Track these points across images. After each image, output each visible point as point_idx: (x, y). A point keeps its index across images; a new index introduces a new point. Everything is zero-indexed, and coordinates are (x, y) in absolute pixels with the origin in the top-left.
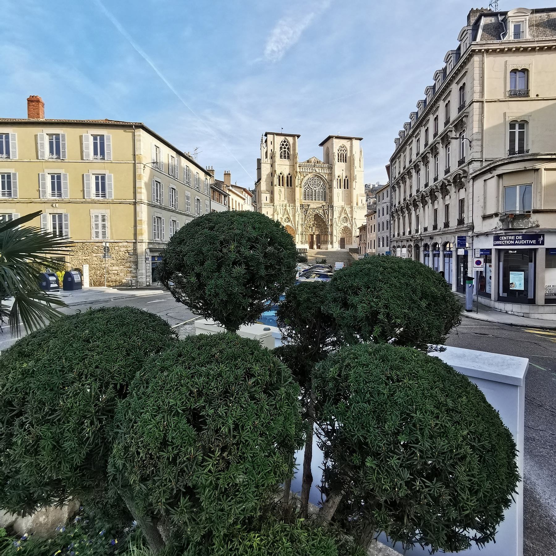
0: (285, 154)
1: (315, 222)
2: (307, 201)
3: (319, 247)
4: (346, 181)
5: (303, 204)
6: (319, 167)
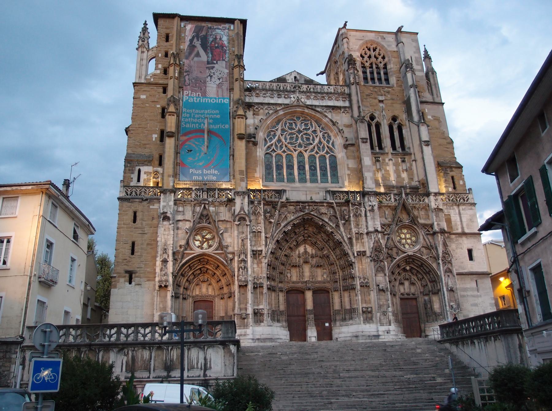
1: (309, 249)
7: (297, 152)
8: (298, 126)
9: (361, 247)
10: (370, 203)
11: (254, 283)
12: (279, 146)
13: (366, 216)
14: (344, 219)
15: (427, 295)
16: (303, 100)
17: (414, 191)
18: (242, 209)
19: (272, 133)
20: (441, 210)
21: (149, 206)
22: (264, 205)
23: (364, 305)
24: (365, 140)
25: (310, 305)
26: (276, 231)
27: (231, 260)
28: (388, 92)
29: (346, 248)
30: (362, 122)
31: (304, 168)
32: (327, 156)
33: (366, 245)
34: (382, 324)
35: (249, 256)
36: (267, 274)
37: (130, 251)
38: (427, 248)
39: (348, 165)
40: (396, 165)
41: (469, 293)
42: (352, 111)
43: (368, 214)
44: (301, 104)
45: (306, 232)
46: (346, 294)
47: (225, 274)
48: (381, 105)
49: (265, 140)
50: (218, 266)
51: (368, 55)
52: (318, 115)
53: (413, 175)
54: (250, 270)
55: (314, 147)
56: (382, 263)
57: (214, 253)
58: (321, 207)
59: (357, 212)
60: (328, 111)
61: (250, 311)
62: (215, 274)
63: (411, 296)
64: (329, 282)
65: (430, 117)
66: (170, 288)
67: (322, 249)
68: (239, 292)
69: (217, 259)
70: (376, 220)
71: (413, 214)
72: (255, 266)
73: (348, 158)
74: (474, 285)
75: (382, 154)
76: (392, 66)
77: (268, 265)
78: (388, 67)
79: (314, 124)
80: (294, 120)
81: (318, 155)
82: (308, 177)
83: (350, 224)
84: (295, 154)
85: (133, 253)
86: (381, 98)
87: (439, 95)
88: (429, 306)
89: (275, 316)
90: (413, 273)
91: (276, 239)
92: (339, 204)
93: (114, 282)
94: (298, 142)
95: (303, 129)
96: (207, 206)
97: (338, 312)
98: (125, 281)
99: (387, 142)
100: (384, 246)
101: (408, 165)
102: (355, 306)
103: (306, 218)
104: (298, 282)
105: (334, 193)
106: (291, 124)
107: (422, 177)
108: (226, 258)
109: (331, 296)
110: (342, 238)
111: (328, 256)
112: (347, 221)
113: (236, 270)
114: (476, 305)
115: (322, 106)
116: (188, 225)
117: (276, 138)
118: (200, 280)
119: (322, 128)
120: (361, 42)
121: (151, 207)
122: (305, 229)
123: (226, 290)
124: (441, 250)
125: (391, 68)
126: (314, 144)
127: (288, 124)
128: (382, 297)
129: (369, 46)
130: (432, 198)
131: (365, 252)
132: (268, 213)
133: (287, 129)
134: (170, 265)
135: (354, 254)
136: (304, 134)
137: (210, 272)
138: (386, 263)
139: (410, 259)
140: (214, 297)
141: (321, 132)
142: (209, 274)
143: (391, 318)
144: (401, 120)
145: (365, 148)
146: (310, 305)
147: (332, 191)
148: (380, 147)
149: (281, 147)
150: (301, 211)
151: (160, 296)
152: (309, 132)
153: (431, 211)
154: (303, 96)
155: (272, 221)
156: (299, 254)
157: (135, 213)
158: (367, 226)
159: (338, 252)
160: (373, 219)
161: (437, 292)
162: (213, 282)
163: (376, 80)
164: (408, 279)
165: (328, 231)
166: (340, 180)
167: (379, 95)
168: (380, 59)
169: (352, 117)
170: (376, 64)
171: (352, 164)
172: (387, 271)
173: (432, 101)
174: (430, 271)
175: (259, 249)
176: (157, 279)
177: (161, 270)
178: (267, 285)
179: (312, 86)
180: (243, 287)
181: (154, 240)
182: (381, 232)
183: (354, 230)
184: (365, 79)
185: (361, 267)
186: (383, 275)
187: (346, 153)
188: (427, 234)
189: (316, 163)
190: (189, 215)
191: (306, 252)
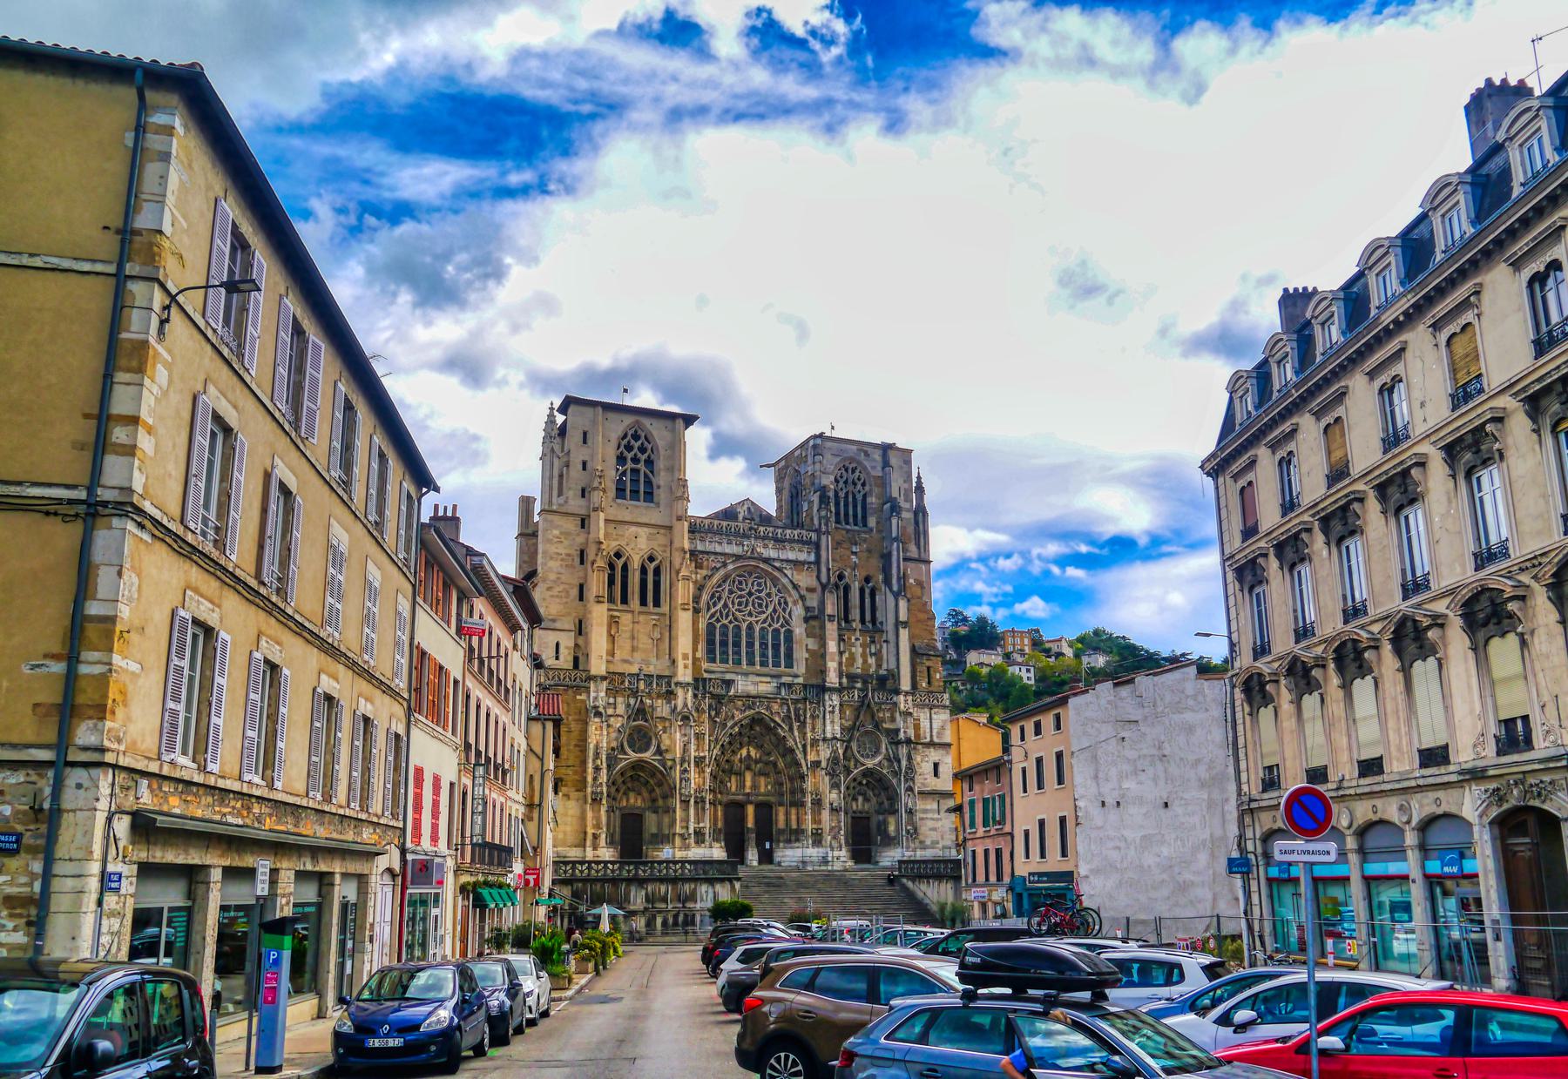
0: (635, 481)
1: (753, 753)
3: (766, 857)
4: (867, 591)
5: (706, 675)
6: (764, 538)
11: (696, 797)
17: (882, 681)
18: (685, 705)
20: (911, 714)
25: (750, 823)
30: (831, 592)
33: (822, 753)
38: (889, 760)
40: (863, 646)
41: (930, 816)
42: (819, 571)
43: (828, 716)
46: (793, 811)
52: (776, 574)
61: (691, 830)
65: (911, 581)
66: (604, 802)
73: (808, 636)
74: (935, 806)
78: (869, 500)
82: (757, 659)
84: (744, 626)
87: (926, 550)
92: (796, 701)
97: (781, 832)
99: (855, 614)
105: (790, 686)
106: (740, 583)
107: (893, 666)
114: (934, 829)
116: (617, 723)
117: (722, 602)
119: (779, 591)
120: (838, 459)
122: (752, 729)
123: (660, 802)
124: (904, 763)
129: (847, 464)
130: (902, 698)
131: (819, 762)
133: (735, 589)
134: (604, 772)
139: (868, 773)
140: (644, 810)
143: (843, 842)
145: (831, 629)
146: (750, 823)
148: (847, 620)
149: (727, 616)
152: (763, 595)
159: (789, 758)
160: (832, 722)
161: (894, 812)
163: (851, 520)
166: (795, 664)
168: (859, 484)
169: (818, 577)
171: (812, 644)
173: (917, 556)
176: (589, 790)
177: (595, 779)
179: (771, 529)
180: (685, 803)
183: (809, 735)
184: (837, 514)
190: (621, 709)
191: (749, 755)
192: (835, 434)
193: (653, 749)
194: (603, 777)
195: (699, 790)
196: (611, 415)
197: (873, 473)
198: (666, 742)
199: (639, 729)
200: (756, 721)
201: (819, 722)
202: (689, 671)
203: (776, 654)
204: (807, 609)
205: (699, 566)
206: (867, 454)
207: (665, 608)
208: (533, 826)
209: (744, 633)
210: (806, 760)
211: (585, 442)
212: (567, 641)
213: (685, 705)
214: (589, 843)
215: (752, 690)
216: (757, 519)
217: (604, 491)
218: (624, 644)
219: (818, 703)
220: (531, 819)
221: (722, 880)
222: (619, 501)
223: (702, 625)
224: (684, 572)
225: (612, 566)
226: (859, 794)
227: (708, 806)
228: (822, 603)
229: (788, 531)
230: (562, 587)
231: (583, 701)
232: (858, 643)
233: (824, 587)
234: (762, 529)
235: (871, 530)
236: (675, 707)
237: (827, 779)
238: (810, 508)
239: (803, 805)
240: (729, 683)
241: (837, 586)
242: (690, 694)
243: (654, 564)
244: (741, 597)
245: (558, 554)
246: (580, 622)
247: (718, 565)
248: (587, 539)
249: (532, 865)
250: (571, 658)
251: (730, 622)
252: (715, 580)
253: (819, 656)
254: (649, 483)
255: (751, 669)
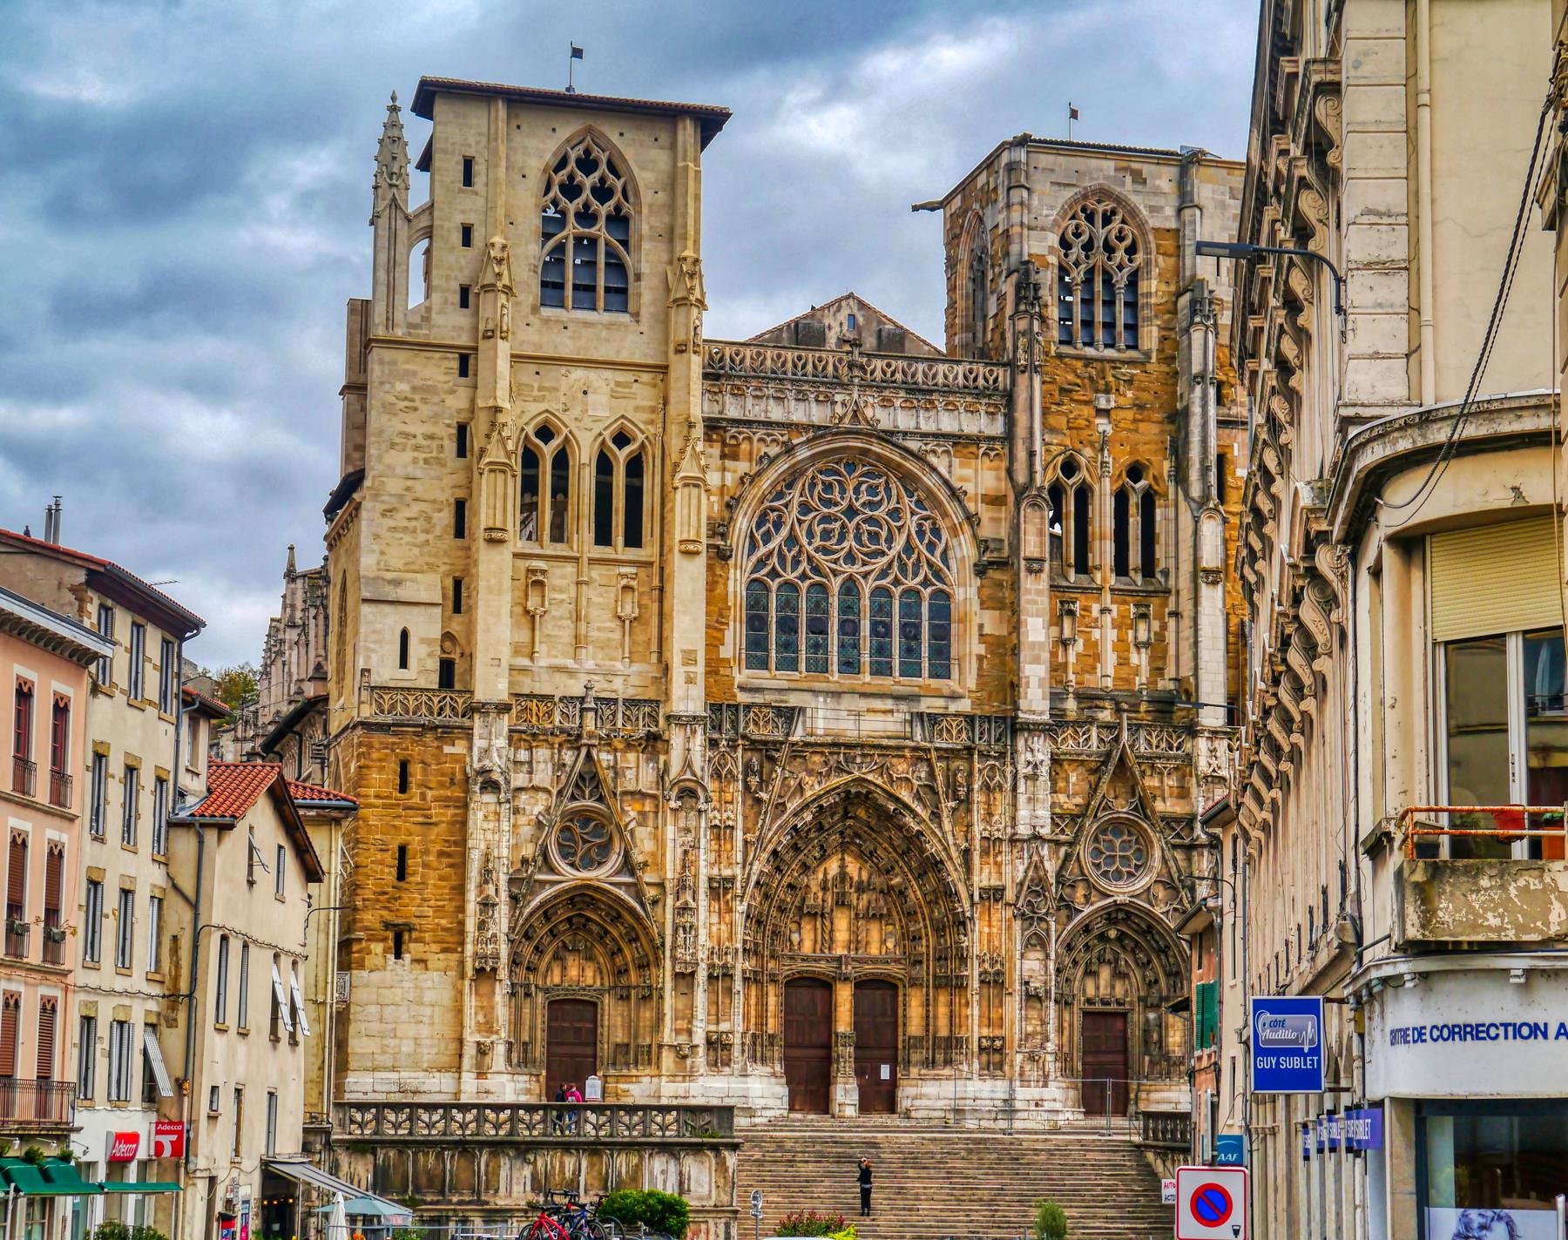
1: (853, 868)
2: (770, 677)
3: (880, 1098)
4: (1134, 500)
5: (743, 698)
7: (840, 579)
8: (850, 493)
9: (994, 876)
10: (1029, 757)
11: (712, 966)
12: (789, 556)
13: (1014, 788)
14: (956, 798)
15: (1155, 1007)
16: (869, 413)
18: (688, 764)
19: (773, 516)
20: (1223, 779)
21: (440, 748)
22: (744, 750)
23: (985, 1032)
24: (1036, 566)
25: (844, 1022)
26: (773, 821)
27: (655, 902)
28: (1130, 382)
29: (955, 875)
31: (856, 629)
32: (926, 592)
33: (1007, 869)
34: (1025, 1082)
35: (702, 896)
36: (745, 942)
37: (394, 871)
38: (1170, 886)
39: (981, 626)
42: (1012, 457)
43: (1021, 788)
44: (863, 426)
45: (849, 822)
46: (943, 998)
47: (636, 939)
48: (1102, 424)
49: (752, 536)
50: (619, 916)
51: (1085, 238)
52: (911, 466)
53: (1164, 658)
54: (703, 932)
55: (890, 565)
56: (1044, 925)
57: (611, 884)
58: (895, 761)
59: (992, 779)
60: (940, 450)
61: (699, 1038)
62: (607, 932)
63: (1113, 1007)
64: (897, 961)
66: (503, 974)
67: (888, 872)
68: (675, 988)
69: (618, 899)
70: (1038, 806)
71: (1144, 789)
72: (715, 919)
73: (983, 606)
75: (1084, 590)
76: (1154, 283)
77: (748, 916)
78: (1143, 286)
79: (896, 486)
80: (839, 474)
81: (900, 588)
82: (866, 658)
83: (969, 811)
84: (836, 584)
85: (401, 875)
86: (1103, 404)
88: (1155, 1036)
89: (758, 1048)
90: (1124, 948)
91: (770, 847)
92: (948, 754)
93: (359, 952)
94: (845, 544)
95: (864, 505)
96: (594, 752)
97: (918, 1042)
98: (385, 951)
99: (1103, 551)
100: (1052, 880)
101: (1156, 625)
102: (963, 1034)
103: (853, 790)
104: (816, 960)
105: (933, 719)
106: (828, 487)
107: (1186, 672)
108: (639, 897)
109: (900, 998)
110: (945, 849)
111: (901, 892)
112: (961, 801)
113: (669, 931)
115: (925, 435)
117: (784, 532)
118: (565, 947)
119: (919, 503)
120: (1068, 194)
121: (447, 749)
122: (846, 816)
123: (633, 977)
125: (1149, 295)
126: (892, 553)
127: (820, 487)
128: (1034, 1014)
129: (1091, 204)
130: (1202, 744)
131: (1003, 889)
132: (754, 773)
133: (815, 503)
135: (972, 896)
136: (865, 521)
137: (595, 928)
138: (1053, 924)
139: (1118, 914)
140: (601, 992)
141: (913, 513)
142: (590, 932)
143: (1051, 1065)
144: (1154, 477)
145: (1035, 593)
146: (844, 1022)
147: (929, 715)
148: (1082, 566)
150: (843, 771)
151: (477, 993)
152: (880, 513)
153: (1194, 780)
154: (870, 400)
155: (764, 796)
156: (825, 881)
157: (404, 766)
158: (1014, 818)
159: (931, 881)
160: (1032, 800)
162: (599, 950)
163: (1100, 335)
164: (1109, 962)
165: (909, 829)
167: (1097, 391)
168: (1120, 255)
169: (1010, 472)
170: (1105, 272)
171: (991, 622)
172: (1053, 949)
174: (1168, 947)
175: (727, 873)
176: (469, 949)
177: (482, 926)
178: (744, 972)
179: (901, 364)
181: (456, 843)
182: (1049, 841)
183: (978, 829)
185: (986, 930)
186: (1040, 955)
187: (980, 589)
188: (1175, 847)
189: (890, 615)
190: (544, 775)
191: (843, 875)
192: (1081, 133)
193: (615, 860)
194: (502, 919)
195: (718, 951)
196: (526, 118)
197: (1153, 222)
198: (644, 846)
199: (584, 817)
200: (854, 799)
201: (1001, 802)
202: (698, 691)
203: (910, 651)
204: (983, 545)
205: (730, 454)
206: (1139, 178)
207: (648, 551)
208: (175, 1037)
209: (835, 601)
210: (969, 887)
211: (468, 181)
212: (427, 628)
213: (688, 764)
214: (467, 1062)
215: (848, 728)
216: (870, 342)
217: (508, 290)
218: (556, 627)
219: (1002, 755)
220: (171, 1023)
221: (697, 1149)
222: (547, 312)
223: (736, 583)
224: (688, 469)
225: (530, 459)
226: (1101, 960)
227: (738, 985)
228: (1016, 529)
229: (942, 368)
230: (416, 508)
231: (456, 758)
232: (1108, 618)
233: (1020, 493)
234: (879, 364)
235: (1148, 355)
236: (666, 770)
237: (1017, 925)
238: (1001, 309)
239: (959, 985)
240: (789, 715)
241: (1056, 492)
242: (699, 739)
243: (628, 449)
244: (827, 519)
245: (406, 435)
246: (458, 584)
247: (774, 450)
248: (473, 401)
249: (173, 1114)
250: (434, 665)
251: (804, 577)
252: (765, 483)
253: (1006, 651)
254: (617, 266)
255: (849, 681)
